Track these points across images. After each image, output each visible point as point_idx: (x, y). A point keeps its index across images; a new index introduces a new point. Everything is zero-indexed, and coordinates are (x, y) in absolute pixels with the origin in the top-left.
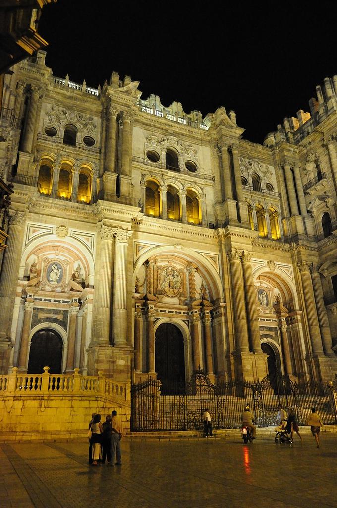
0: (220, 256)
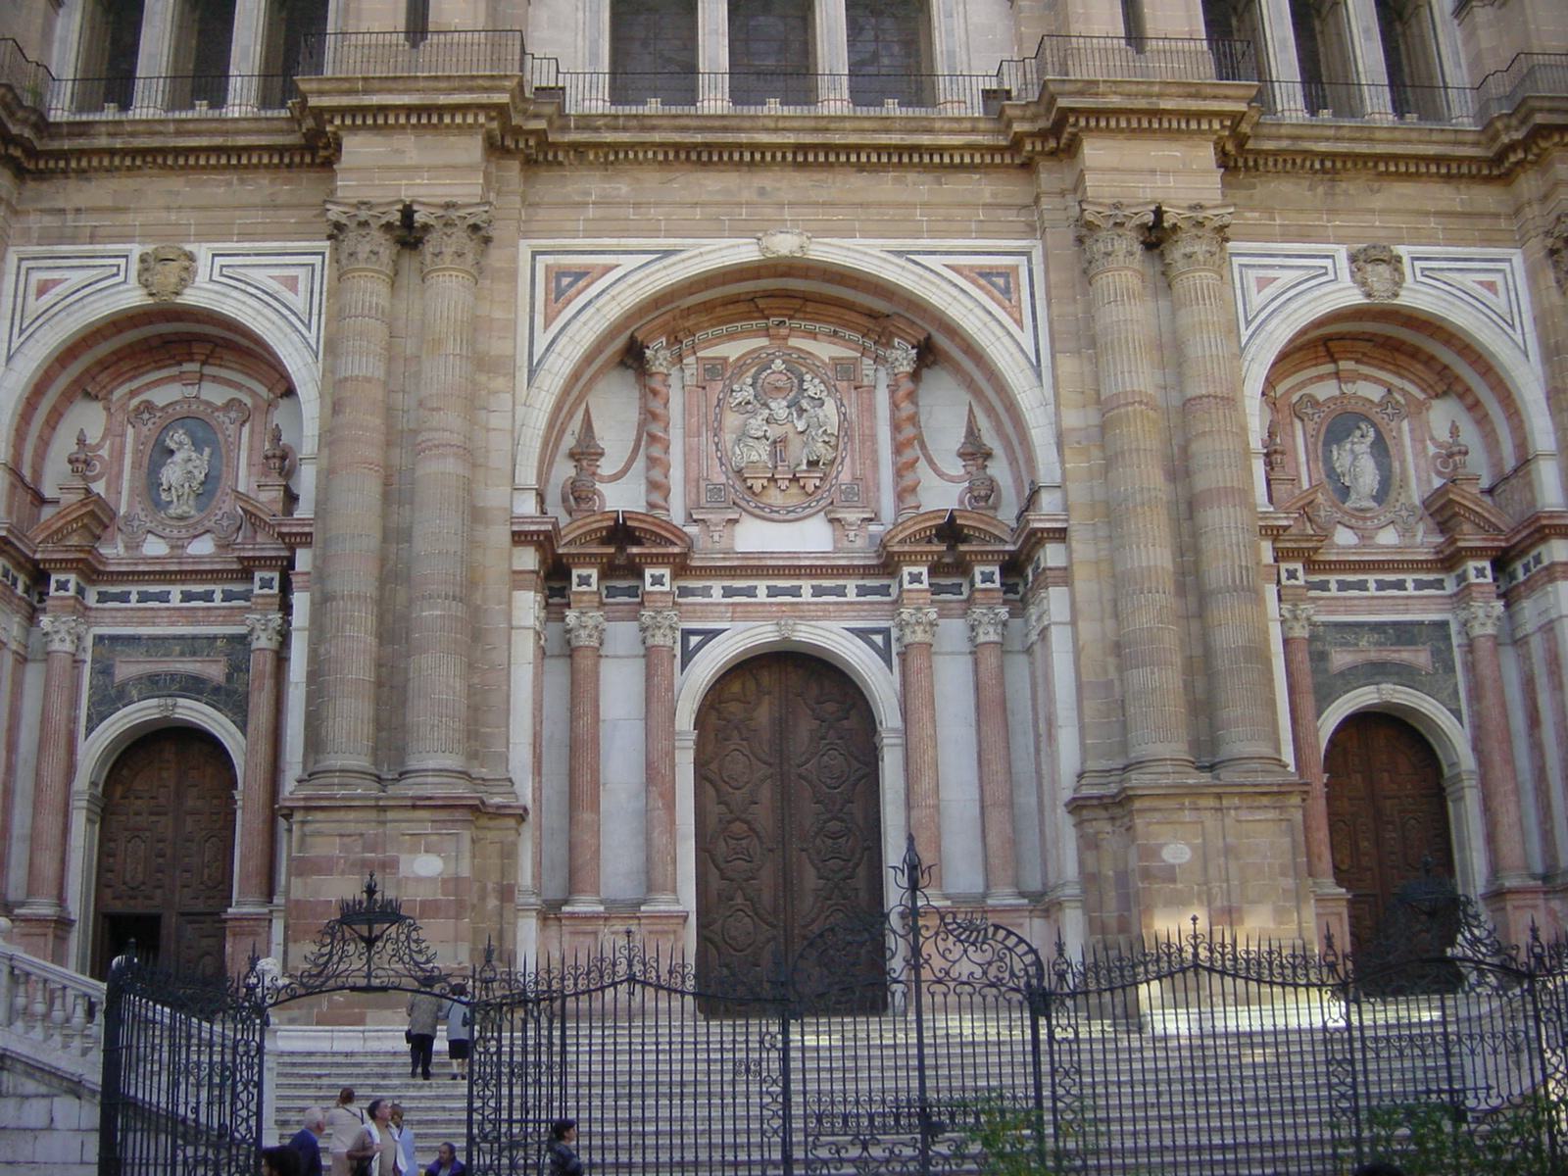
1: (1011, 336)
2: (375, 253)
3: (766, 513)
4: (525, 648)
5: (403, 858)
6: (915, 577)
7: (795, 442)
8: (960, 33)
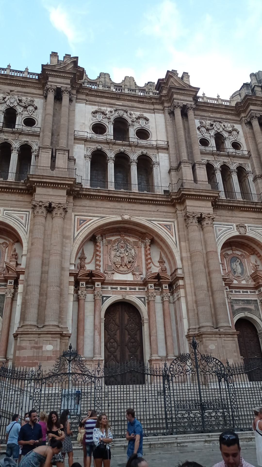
0: (176, 223)
1: (171, 238)
2: (43, 212)
3: (120, 272)
4: (71, 298)
5: (44, 346)
6: (151, 286)
7: (126, 258)
8: (159, 179)
